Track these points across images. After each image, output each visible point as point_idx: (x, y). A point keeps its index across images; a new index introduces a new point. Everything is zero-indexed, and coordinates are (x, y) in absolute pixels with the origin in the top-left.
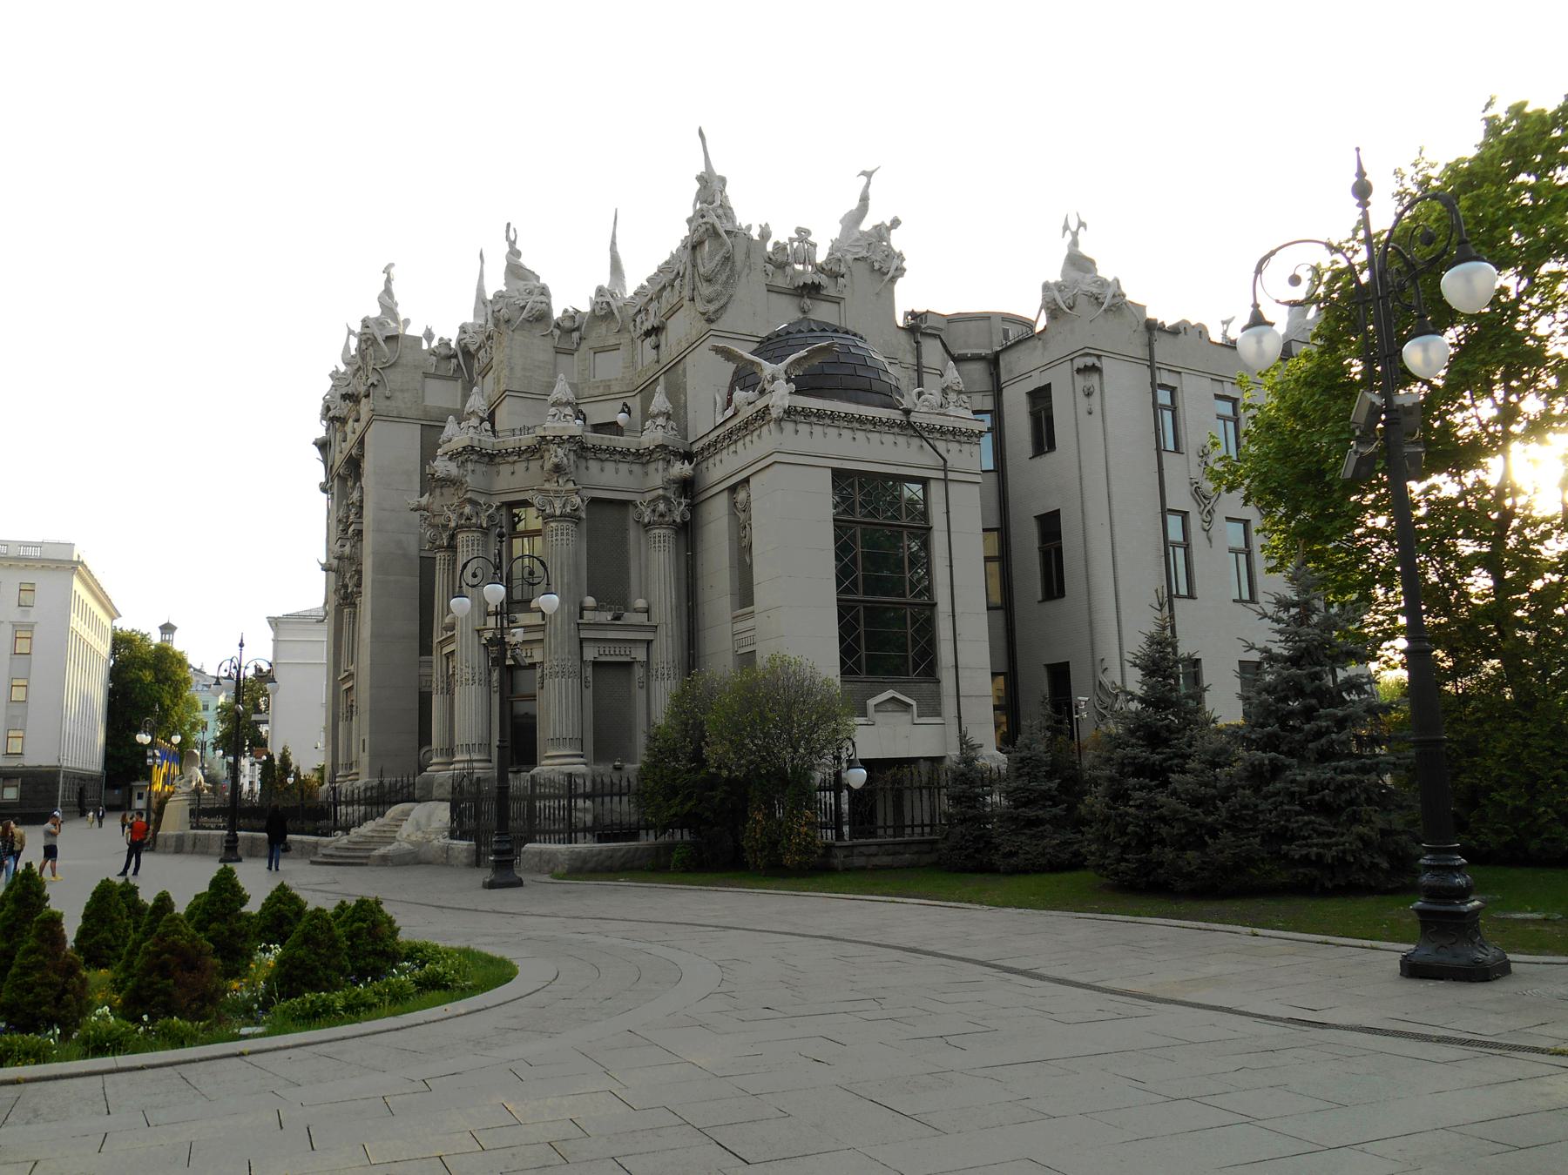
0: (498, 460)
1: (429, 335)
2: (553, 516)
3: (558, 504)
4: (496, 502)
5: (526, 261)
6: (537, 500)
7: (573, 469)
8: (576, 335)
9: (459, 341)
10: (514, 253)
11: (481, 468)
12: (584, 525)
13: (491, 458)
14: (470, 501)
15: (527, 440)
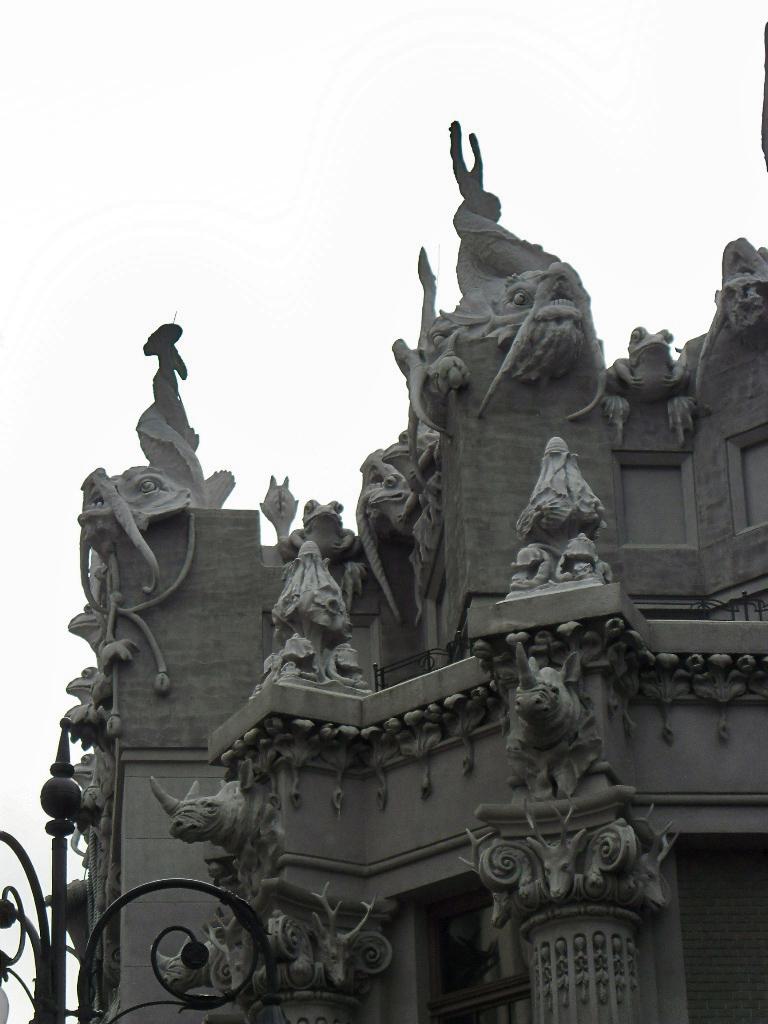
0: (379, 757)
1: (279, 502)
2: (544, 903)
3: (556, 857)
4: (374, 898)
5: (514, 221)
6: (485, 861)
7: (600, 732)
8: (680, 406)
9: (365, 506)
10: (477, 207)
11: (323, 791)
12: (673, 942)
13: (355, 755)
14: (285, 898)
15: (467, 670)
